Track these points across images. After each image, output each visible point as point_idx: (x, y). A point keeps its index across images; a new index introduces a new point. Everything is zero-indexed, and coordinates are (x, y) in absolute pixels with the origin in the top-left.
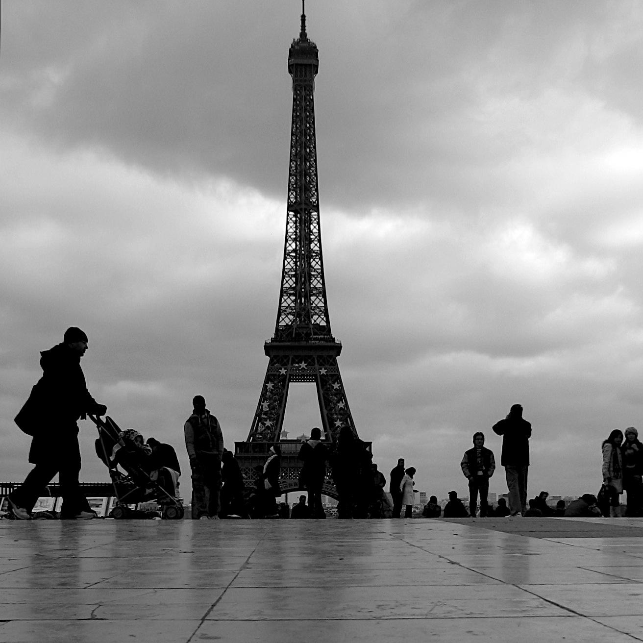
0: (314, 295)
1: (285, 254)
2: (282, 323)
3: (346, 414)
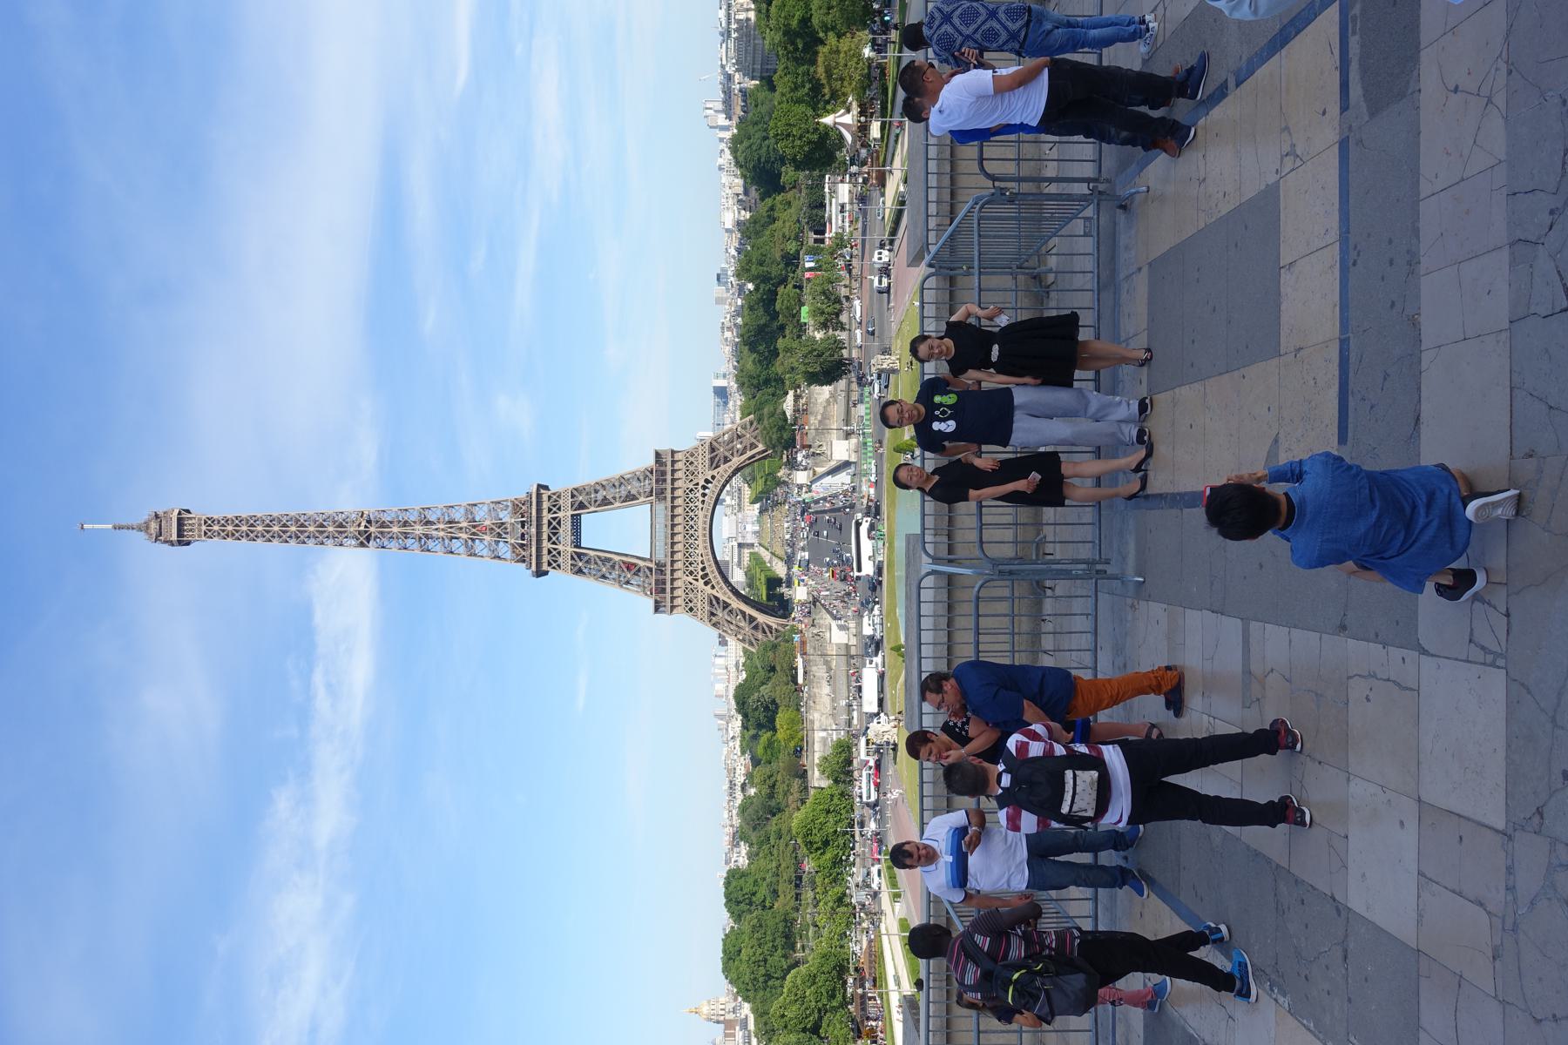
2: (508, 555)
3: (623, 481)
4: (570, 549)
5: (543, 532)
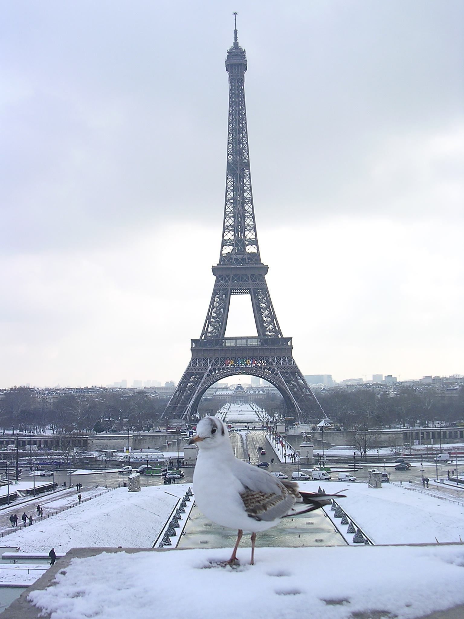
0: (248, 230)
1: (226, 201)
3: (273, 317)
4: (229, 288)
5: (240, 272)
